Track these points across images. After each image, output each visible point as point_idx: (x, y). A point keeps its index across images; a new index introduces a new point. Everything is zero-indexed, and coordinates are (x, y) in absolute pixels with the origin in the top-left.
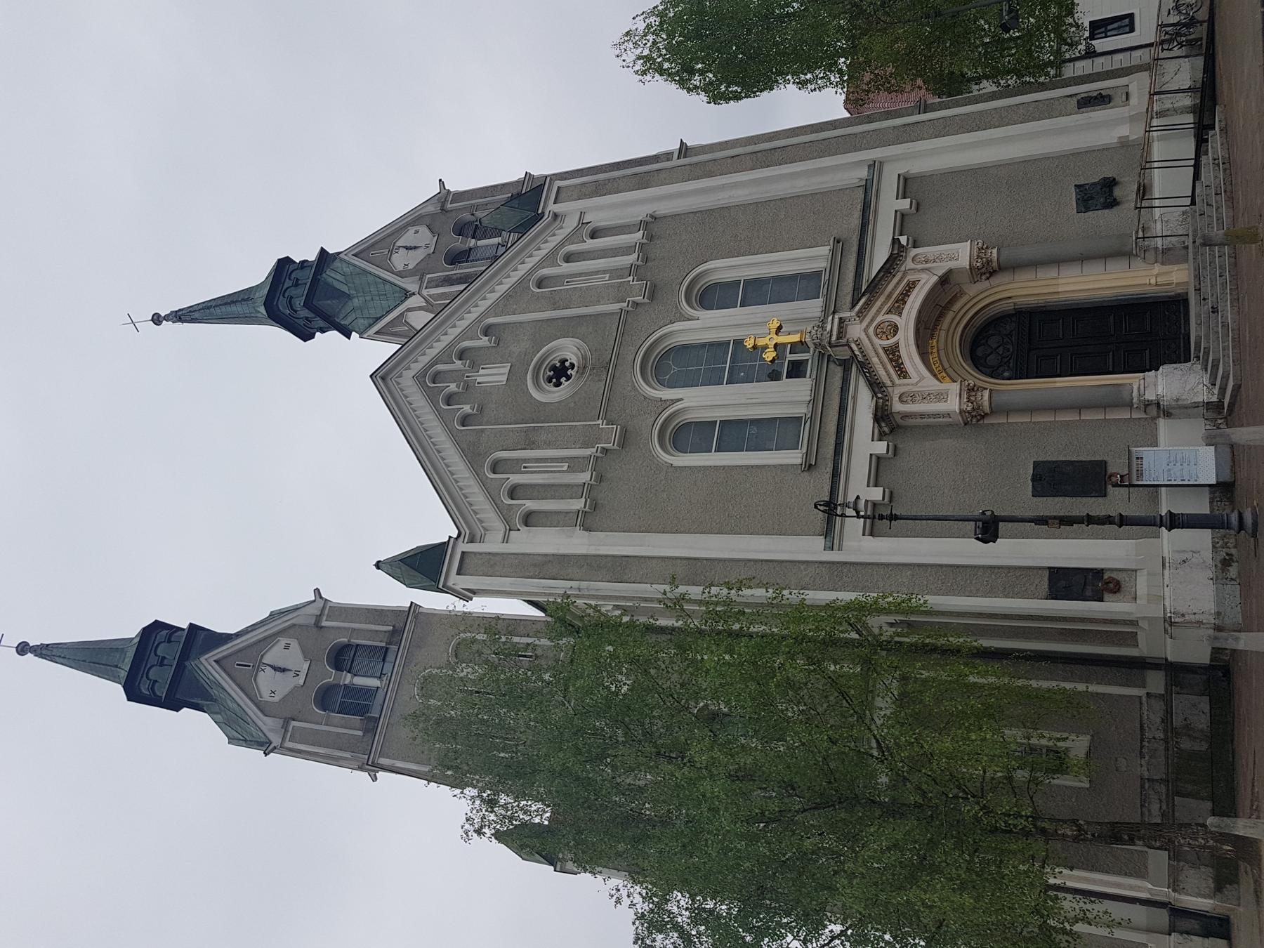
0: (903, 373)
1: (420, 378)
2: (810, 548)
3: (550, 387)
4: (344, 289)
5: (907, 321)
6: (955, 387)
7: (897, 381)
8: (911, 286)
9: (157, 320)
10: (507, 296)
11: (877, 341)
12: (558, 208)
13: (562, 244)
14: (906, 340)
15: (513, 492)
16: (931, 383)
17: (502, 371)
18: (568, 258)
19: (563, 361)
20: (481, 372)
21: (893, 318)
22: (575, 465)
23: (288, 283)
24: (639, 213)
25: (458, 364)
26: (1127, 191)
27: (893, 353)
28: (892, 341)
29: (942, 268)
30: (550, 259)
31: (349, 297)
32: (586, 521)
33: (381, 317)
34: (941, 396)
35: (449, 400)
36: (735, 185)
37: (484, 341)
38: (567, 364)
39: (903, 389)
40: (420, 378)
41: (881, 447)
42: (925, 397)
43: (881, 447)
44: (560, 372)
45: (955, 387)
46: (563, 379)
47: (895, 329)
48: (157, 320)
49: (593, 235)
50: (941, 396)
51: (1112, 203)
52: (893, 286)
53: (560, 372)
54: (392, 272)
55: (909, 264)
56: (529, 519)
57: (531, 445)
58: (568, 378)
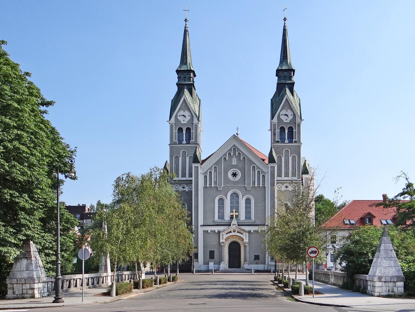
0: (227, 234)
1: (234, 146)
2: (201, 222)
3: (232, 173)
4: (280, 95)
5: (236, 234)
6: (224, 241)
7: (225, 233)
8: (242, 234)
9: (285, 19)
10: (251, 161)
11: (233, 229)
12: (269, 167)
13: (261, 170)
14: (233, 234)
15: (211, 172)
16: (224, 238)
17: (235, 162)
18: (259, 172)
19: (237, 175)
20: (235, 158)
21: (236, 232)
22: (215, 183)
23: (286, 73)
24: (266, 185)
25: (237, 154)
26: (257, 261)
27: (231, 232)
28: (232, 232)
29: (244, 238)
30: (258, 168)
31: (279, 96)
32: (205, 187)
33: (272, 108)
34: (223, 239)
35: (230, 153)
36: (268, 202)
37: (242, 158)
38: (236, 176)
39: (224, 234)
40: (234, 146)
41: (216, 231)
42: (223, 237)
43: (216, 231)
44: (234, 175)
45: (224, 241)
46: (233, 176)
47: (234, 232)
48: (285, 19)
49: (264, 176)
50: (223, 239)
51: (255, 259)
52: (242, 232)
53: (234, 175)
54: (280, 112)
55: (245, 233)
56: (206, 177)
57: (219, 174)
58: (233, 177)
